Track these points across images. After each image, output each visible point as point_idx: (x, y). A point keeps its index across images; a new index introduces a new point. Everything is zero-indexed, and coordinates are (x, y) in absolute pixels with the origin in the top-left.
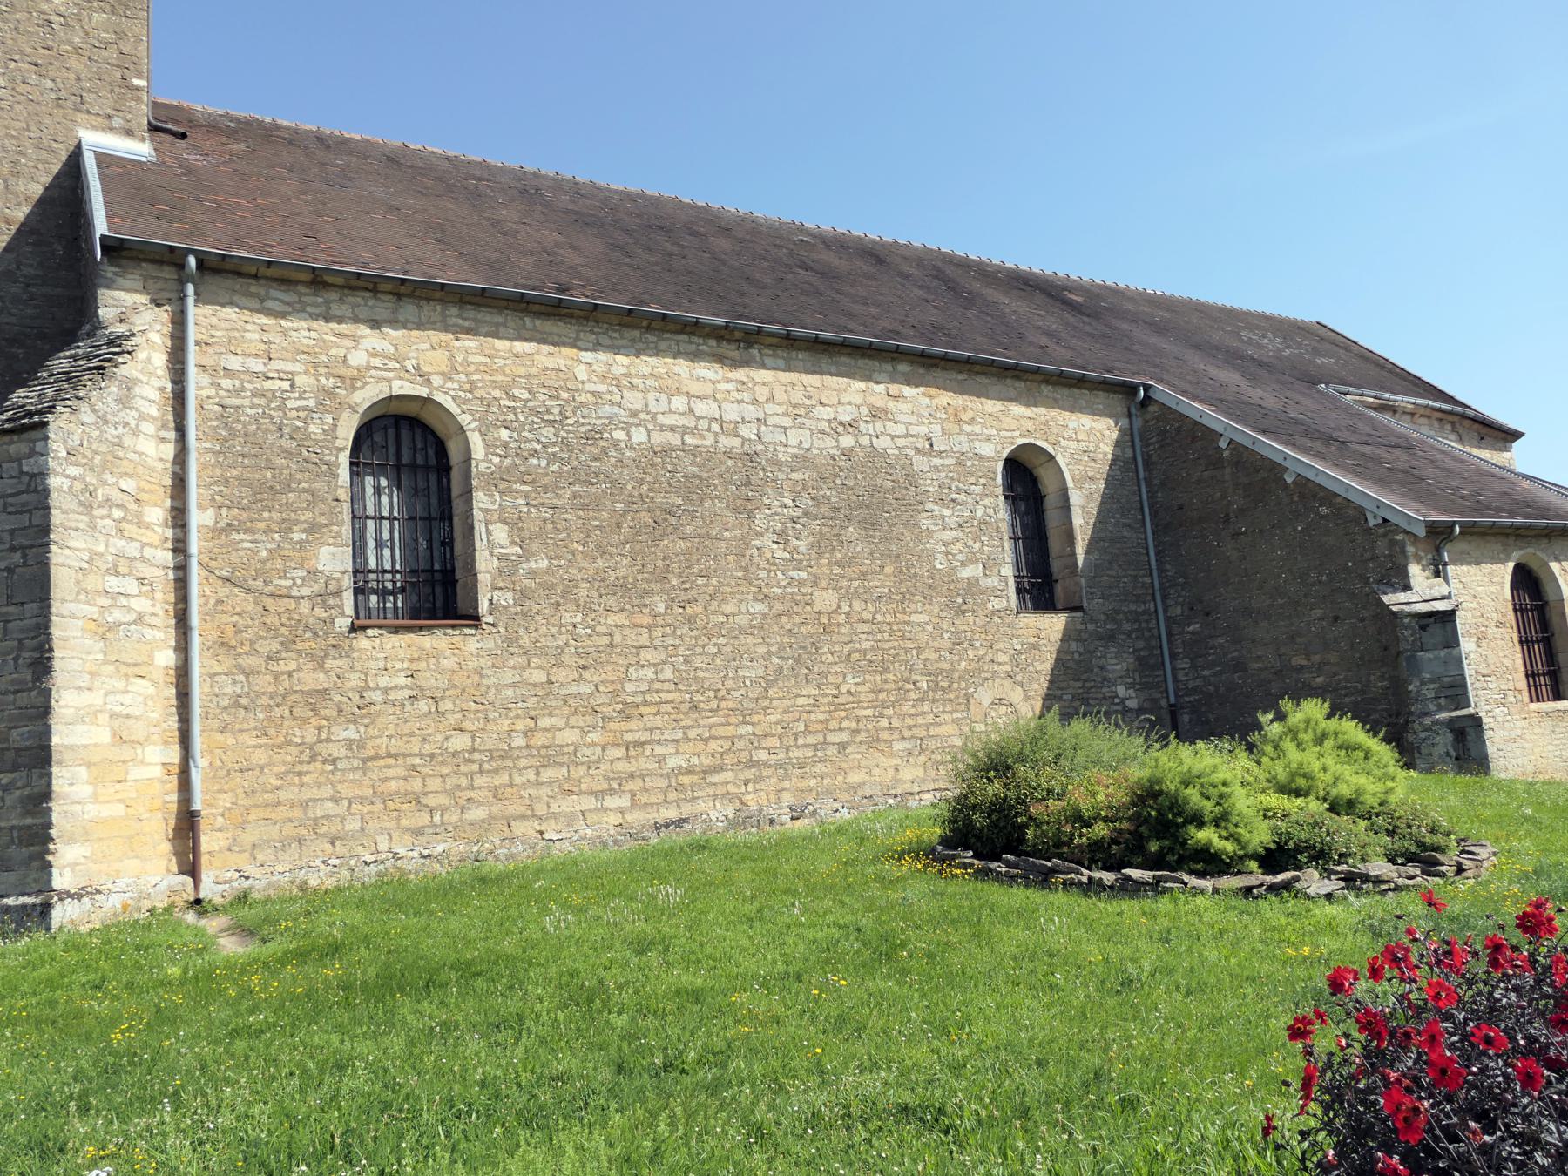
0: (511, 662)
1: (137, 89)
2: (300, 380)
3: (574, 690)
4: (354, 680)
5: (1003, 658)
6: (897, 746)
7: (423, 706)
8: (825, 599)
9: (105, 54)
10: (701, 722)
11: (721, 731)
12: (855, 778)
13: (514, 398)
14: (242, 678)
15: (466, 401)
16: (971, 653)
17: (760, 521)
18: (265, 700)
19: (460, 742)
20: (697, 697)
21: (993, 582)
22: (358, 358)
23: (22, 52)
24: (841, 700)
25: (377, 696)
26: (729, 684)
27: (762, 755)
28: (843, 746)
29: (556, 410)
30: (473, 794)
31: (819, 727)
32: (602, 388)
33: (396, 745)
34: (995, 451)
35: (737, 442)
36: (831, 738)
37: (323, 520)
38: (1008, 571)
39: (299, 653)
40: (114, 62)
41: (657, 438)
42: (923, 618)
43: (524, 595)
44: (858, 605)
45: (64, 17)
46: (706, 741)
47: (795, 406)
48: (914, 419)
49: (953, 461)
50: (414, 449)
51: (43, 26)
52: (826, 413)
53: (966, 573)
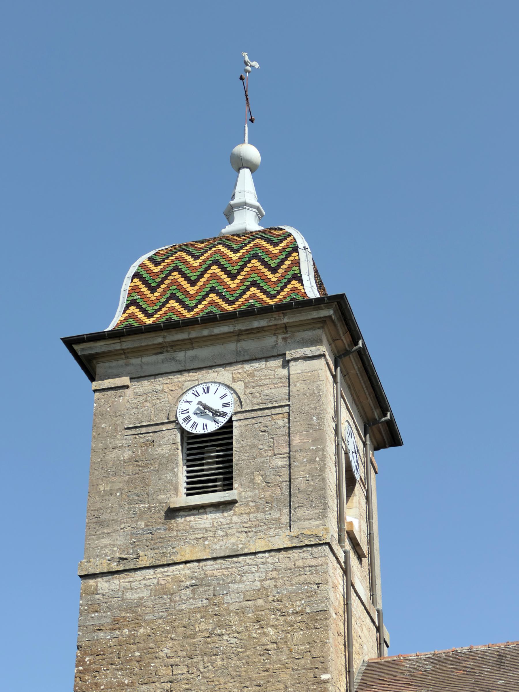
1: (325, 682)
9: (302, 661)
23: (251, 679)
40: (309, 666)
45: (276, 643)
51: (263, 655)
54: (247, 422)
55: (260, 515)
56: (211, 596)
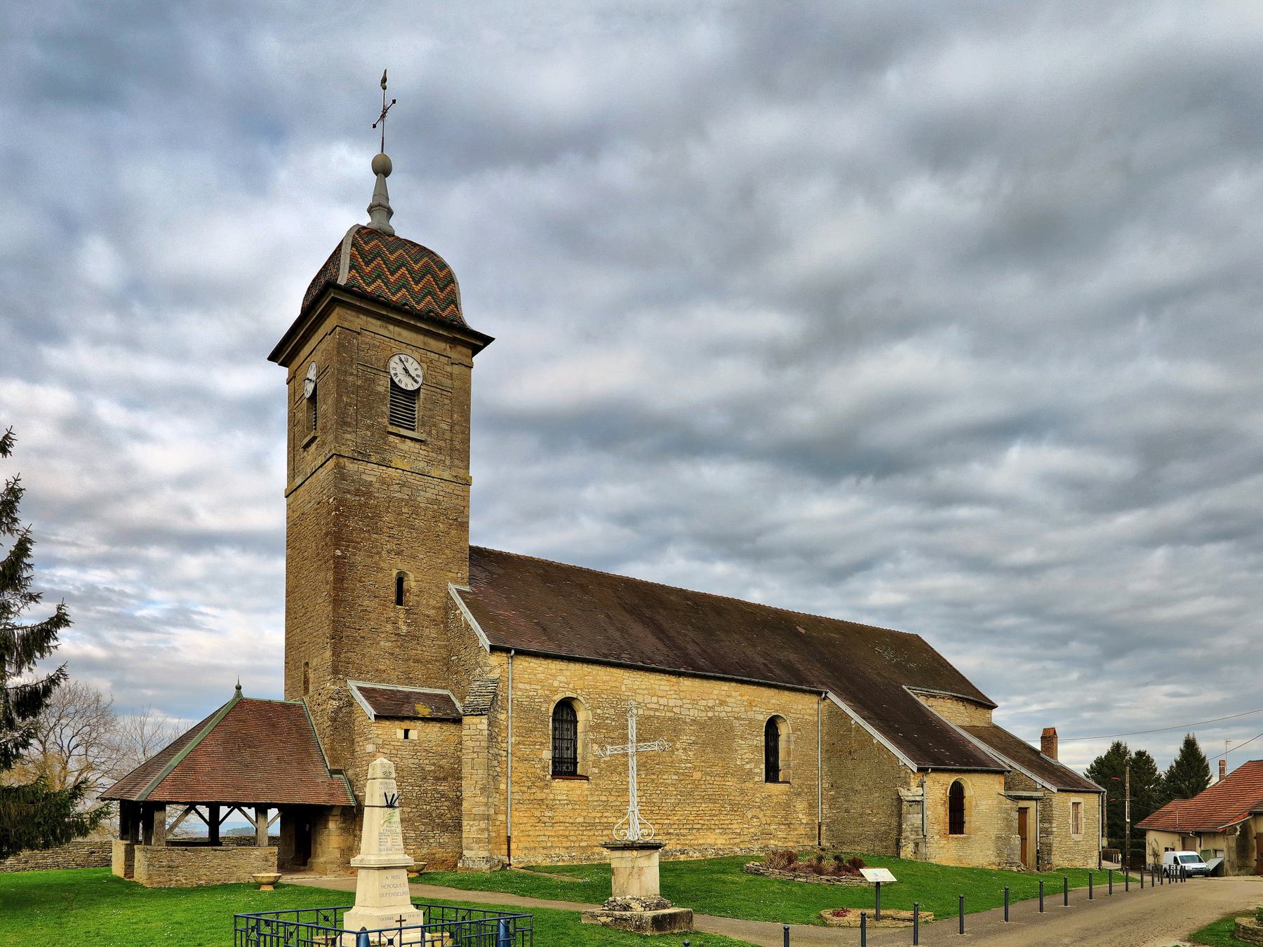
0: (597, 793)
2: (540, 692)
3: (614, 804)
4: (552, 796)
5: (758, 800)
6: (717, 831)
7: (570, 807)
8: (697, 775)
10: (653, 817)
11: (659, 821)
12: (701, 841)
13: (603, 698)
14: (521, 794)
15: (588, 699)
16: (746, 798)
17: (678, 746)
18: (527, 802)
19: (580, 820)
20: (652, 809)
21: (757, 770)
22: (556, 684)
24: (700, 812)
25: (558, 802)
26: (663, 805)
27: (672, 831)
28: (699, 829)
29: (615, 702)
30: (583, 837)
31: (692, 822)
32: (630, 694)
33: (562, 819)
34: (763, 718)
35: (672, 714)
36: (695, 826)
37: (544, 741)
38: (763, 766)
39: (537, 787)
41: (647, 713)
42: (730, 784)
43: (601, 770)
44: (708, 778)
46: (654, 824)
47: (694, 700)
48: (735, 705)
49: (747, 722)
50: (567, 715)
52: (704, 703)
53: (748, 766)
54: (428, 392)
55: (435, 455)
56: (410, 494)
